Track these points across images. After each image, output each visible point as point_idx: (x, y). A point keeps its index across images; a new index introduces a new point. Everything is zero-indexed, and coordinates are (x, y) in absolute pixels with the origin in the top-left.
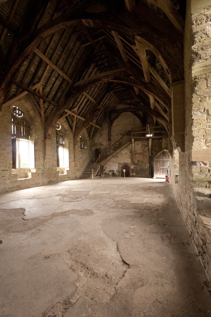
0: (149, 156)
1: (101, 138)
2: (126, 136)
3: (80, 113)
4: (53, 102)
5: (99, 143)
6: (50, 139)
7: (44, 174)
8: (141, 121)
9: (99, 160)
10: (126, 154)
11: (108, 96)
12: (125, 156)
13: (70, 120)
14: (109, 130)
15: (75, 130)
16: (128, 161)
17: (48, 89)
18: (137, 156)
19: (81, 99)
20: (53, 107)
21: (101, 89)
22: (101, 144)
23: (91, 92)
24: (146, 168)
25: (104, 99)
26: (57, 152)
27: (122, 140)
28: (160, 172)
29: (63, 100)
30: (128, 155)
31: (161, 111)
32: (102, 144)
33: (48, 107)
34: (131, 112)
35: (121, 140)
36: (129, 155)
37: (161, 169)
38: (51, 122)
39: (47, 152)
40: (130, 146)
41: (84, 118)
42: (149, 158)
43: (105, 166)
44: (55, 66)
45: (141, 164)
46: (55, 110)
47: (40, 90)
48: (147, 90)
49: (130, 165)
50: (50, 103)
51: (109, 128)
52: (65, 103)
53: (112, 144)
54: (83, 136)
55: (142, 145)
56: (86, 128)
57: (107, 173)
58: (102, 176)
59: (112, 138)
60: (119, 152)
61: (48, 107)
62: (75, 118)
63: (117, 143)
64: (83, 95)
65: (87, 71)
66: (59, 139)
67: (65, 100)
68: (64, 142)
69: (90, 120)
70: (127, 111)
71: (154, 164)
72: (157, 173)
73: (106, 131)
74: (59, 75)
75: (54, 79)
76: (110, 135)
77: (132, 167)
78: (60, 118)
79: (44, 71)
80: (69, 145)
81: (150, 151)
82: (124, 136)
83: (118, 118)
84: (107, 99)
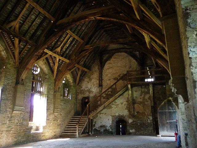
0: (152, 106)
1: (89, 83)
2: (121, 82)
3: (63, 54)
4: (30, 42)
5: (87, 90)
6: (23, 84)
7: (10, 131)
8: (138, 63)
9: (86, 111)
11: (98, 35)
12: (120, 105)
13: (51, 62)
14: (100, 74)
15: (57, 74)
16: (125, 113)
17: (26, 27)
19: (65, 38)
20: (30, 47)
21: (89, 28)
22: (90, 91)
23: (77, 30)
25: (93, 38)
26: (31, 101)
27: (116, 86)
28: (167, 127)
29: (42, 39)
30: (125, 105)
31: (160, 51)
32: (91, 91)
33: (25, 46)
34: (126, 52)
35: (114, 86)
36: (126, 106)
37: (167, 123)
38: (27, 64)
39: (17, 102)
40: (126, 93)
41: (69, 59)
42: (152, 109)
43: (95, 120)
44: (35, 4)
46: (32, 50)
47: (16, 29)
48: (140, 27)
50: (27, 42)
51: (100, 71)
52: (44, 43)
53: (103, 91)
54: (67, 81)
55: (142, 93)
56: (71, 71)
57: (97, 129)
58: (90, 133)
59: (104, 84)
60: (112, 102)
61: (25, 46)
62: (58, 60)
63: (110, 90)
64: (68, 34)
65: (73, 8)
66: (35, 85)
67: (45, 39)
68: (42, 88)
69: (75, 61)
70: (121, 52)
71: (158, 117)
72: (163, 130)
73: (96, 75)
74: (40, 13)
75: (33, 17)
76: (101, 79)
77: (130, 121)
78: (39, 59)
79: (22, 9)
80: (48, 92)
81: (152, 99)
82: (118, 81)
83: (110, 60)
84: (97, 38)
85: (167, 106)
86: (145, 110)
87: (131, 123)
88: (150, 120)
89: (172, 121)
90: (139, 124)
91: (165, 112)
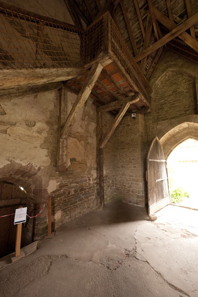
10: (30, 124)
12: (21, 130)
18: (71, 140)
24: (89, 184)
30: (40, 132)
36: (45, 135)
45: (79, 171)
49: (44, 180)
77: (52, 186)
86: (87, 156)
87: (53, 192)
88: (93, 180)
90: (73, 193)
91: (154, 161)
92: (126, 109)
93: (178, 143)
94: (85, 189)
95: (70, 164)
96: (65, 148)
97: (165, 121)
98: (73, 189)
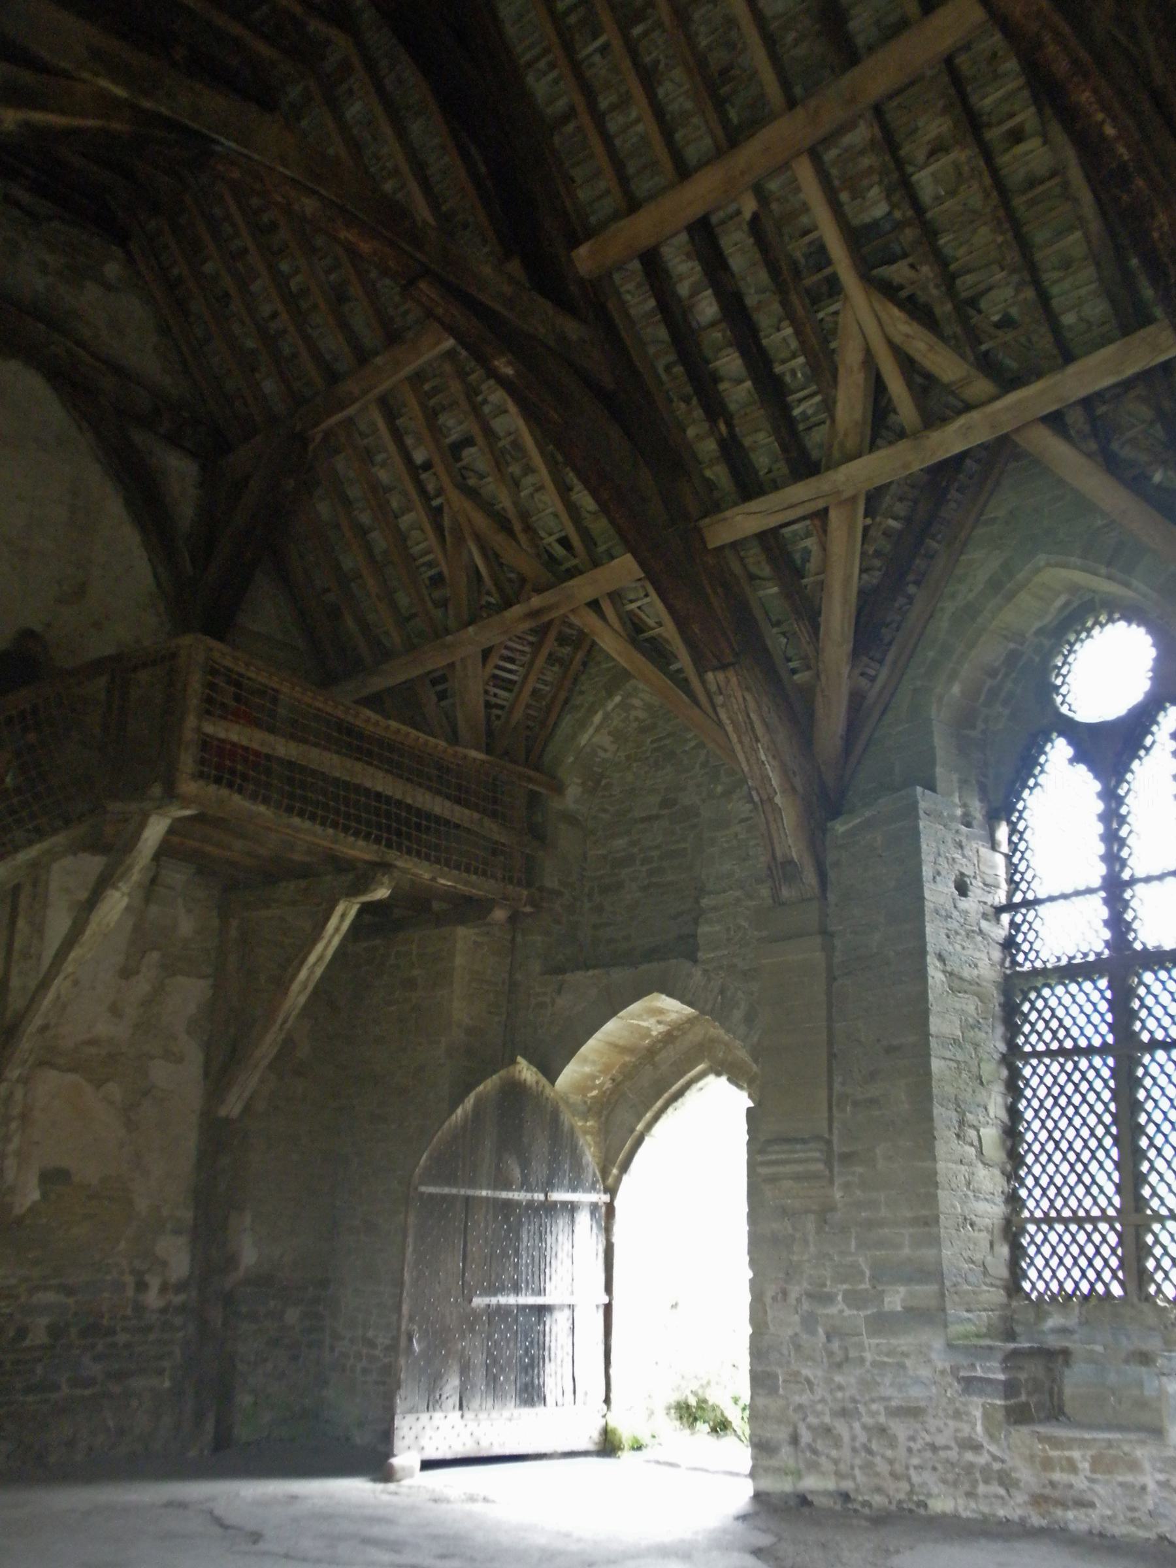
28: (465, 1370)
85: (488, 1144)
88: (164, 1288)
89: (510, 1300)
91: (467, 1199)
92: (337, 929)
93: (666, 1095)
94: (111, 1332)
95: (36, 1195)
96: (14, 1125)
97: (590, 973)
98: (44, 1321)
